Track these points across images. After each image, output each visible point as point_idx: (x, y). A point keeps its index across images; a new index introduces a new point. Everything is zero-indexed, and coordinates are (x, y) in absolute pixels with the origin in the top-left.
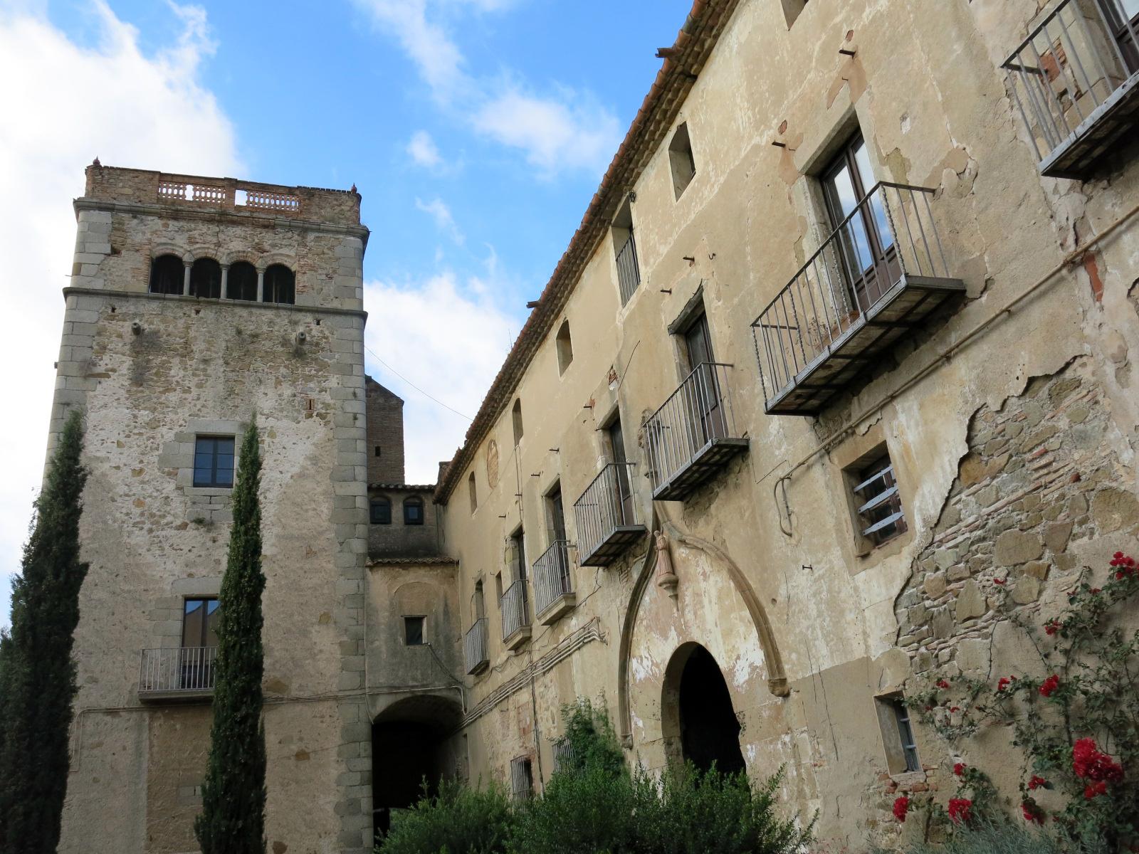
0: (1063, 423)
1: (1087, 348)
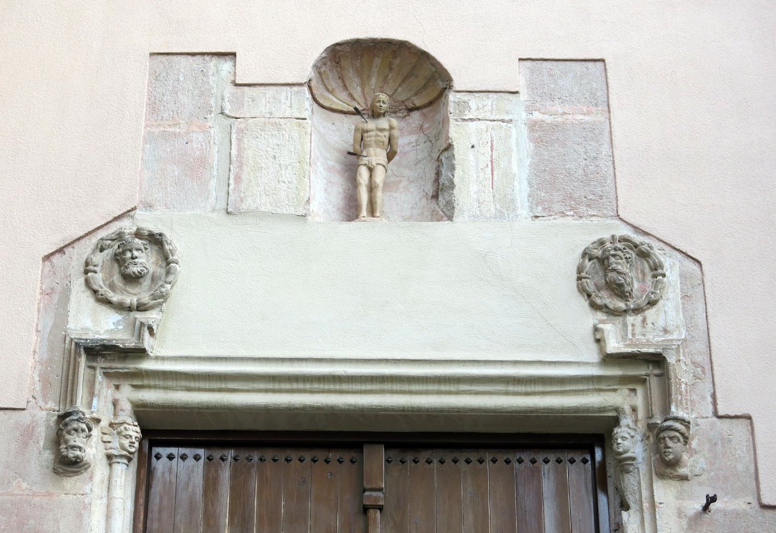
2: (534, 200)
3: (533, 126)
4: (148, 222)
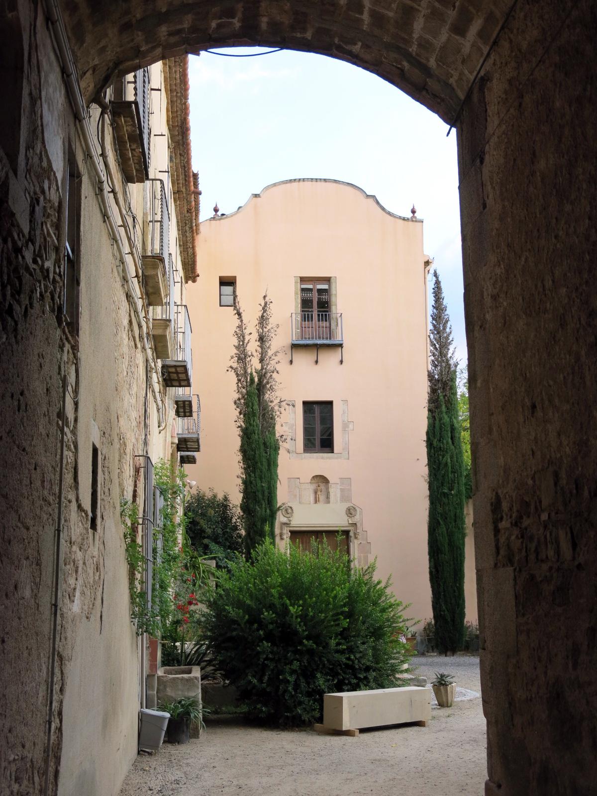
2: (341, 500)
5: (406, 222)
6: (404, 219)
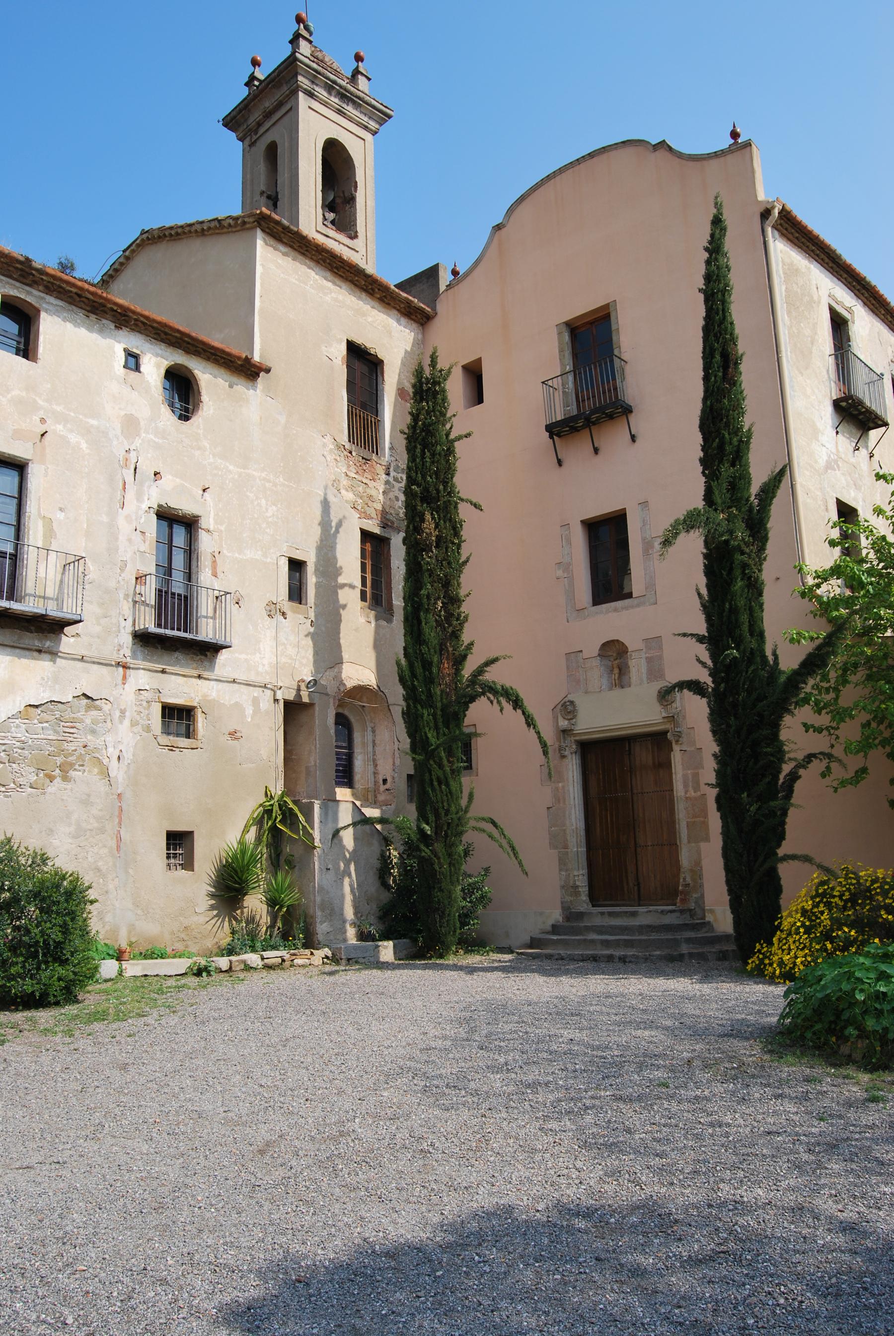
0: (88, 721)
1: (111, 699)
2: (648, 679)
3: (647, 658)
4: (570, 698)
5: (722, 159)
6: (716, 155)
